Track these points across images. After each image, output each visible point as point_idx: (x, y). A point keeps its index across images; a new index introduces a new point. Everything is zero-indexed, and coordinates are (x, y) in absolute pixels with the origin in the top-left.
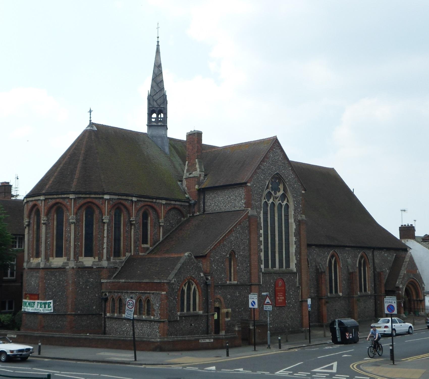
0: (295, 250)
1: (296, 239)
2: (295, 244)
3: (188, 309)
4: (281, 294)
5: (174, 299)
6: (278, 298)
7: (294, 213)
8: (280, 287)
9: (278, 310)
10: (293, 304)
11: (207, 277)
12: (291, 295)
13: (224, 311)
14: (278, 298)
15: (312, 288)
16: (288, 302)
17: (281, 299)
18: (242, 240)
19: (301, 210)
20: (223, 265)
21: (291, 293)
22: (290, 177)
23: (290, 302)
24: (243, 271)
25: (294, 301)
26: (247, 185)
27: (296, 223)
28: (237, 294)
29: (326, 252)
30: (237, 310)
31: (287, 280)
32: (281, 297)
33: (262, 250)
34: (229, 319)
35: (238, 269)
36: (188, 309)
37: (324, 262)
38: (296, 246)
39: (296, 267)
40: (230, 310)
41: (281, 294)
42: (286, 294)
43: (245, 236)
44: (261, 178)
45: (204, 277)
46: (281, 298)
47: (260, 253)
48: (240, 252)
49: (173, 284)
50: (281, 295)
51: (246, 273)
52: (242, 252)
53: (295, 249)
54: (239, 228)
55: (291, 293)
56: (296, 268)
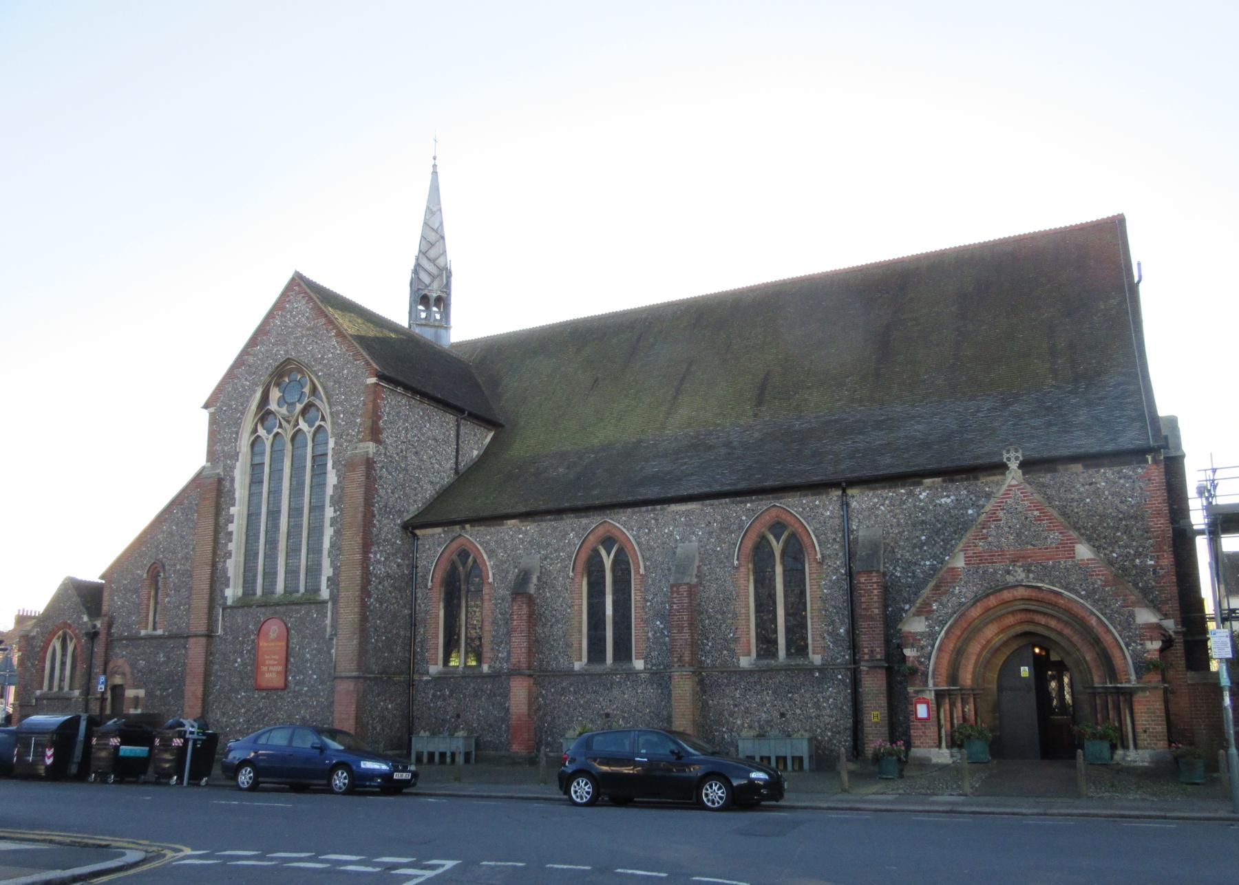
0: (331, 542)
1: (335, 511)
2: (331, 526)
3: (51, 688)
4: (275, 660)
5: (33, 665)
6: (265, 668)
7: (336, 443)
8: (273, 641)
9: (264, 698)
10: (313, 686)
11: (95, 623)
12: (307, 661)
13: (130, 693)
14: (265, 668)
15: (503, 645)
16: (295, 679)
17: (272, 672)
18: (183, 537)
19: (359, 432)
20: (137, 597)
21: (308, 656)
22: (331, 355)
23: (303, 679)
24: (178, 607)
25: (315, 677)
26: (212, 410)
27: (338, 471)
28: (160, 658)
29: (572, 530)
30: (158, 693)
31: (296, 621)
32: (273, 665)
33: (231, 555)
34: (139, 711)
35: (169, 602)
36: (51, 688)
37: (559, 565)
38: (335, 531)
39: (328, 587)
40: (141, 693)
41: (275, 660)
42: (292, 659)
43: (190, 527)
44: (243, 386)
45: (90, 623)
46: (271, 668)
47: (225, 562)
48: (175, 565)
49: (34, 638)
50: (271, 662)
51: (185, 610)
52: (181, 564)
53: (331, 538)
54: (177, 513)
55: (308, 656)
56: (328, 590)
